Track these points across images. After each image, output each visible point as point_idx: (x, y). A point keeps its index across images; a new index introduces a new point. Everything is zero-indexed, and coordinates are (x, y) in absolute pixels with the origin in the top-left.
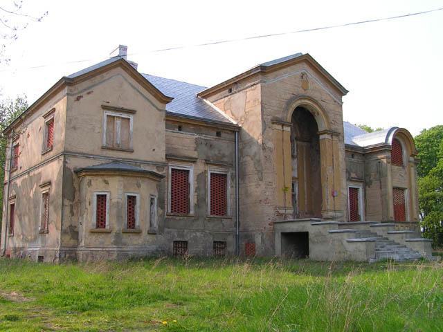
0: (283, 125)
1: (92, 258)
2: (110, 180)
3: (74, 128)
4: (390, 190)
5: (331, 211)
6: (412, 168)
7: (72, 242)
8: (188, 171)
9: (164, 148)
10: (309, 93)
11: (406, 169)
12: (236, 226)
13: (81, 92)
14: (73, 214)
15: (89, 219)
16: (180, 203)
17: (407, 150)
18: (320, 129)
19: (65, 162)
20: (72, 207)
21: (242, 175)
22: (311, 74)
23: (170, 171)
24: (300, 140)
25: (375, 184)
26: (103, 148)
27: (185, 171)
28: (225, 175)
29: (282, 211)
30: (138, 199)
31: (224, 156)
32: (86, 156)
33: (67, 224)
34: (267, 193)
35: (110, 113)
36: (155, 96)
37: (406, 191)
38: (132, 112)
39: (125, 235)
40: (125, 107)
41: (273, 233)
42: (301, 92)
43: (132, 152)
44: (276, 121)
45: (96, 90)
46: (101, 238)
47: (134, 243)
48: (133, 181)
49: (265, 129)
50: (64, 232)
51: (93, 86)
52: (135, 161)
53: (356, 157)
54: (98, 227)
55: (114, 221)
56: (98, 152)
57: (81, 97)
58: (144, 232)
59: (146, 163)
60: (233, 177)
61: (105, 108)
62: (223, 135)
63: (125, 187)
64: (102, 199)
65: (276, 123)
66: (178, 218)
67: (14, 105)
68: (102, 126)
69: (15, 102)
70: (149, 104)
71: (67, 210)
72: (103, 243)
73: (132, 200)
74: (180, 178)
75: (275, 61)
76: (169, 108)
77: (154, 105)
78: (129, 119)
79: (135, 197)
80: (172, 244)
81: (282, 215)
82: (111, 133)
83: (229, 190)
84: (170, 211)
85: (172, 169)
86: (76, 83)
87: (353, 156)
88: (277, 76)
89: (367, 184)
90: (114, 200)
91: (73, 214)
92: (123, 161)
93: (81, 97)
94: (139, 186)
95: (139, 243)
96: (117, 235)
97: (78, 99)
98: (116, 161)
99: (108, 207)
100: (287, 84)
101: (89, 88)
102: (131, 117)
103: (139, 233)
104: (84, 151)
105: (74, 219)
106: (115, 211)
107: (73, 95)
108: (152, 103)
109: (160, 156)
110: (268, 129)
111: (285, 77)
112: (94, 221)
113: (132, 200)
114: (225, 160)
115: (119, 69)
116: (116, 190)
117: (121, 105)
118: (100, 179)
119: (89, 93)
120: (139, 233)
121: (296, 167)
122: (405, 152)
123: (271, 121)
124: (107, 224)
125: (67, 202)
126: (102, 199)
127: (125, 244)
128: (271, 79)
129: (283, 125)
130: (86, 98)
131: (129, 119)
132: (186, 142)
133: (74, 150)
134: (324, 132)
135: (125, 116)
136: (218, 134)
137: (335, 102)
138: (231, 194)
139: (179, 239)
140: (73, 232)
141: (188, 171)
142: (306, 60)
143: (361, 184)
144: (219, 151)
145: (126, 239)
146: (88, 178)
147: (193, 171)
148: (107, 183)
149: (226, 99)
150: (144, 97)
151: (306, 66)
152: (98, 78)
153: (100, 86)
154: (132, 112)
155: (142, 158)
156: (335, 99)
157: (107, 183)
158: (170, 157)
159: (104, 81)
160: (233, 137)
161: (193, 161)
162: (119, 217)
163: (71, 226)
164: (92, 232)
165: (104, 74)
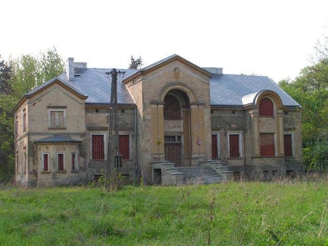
0: (157, 105)
1: (43, 186)
2: (49, 146)
3: (33, 120)
4: (256, 136)
5: (197, 154)
6: (280, 118)
7: (34, 178)
8: (103, 135)
9: (84, 125)
10: (180, 80)
11: (276, 119)
12: (135, 165)
13: (35, 101)
14: (34, 164)
15: (41, 166)
16: (98, 153)
17: (276, 104)
18: (191, 102)
19: (29, 138)
20: (33, 160)
21: (136, 137)
22: (182, 67)
23: (91, 137)
24: (184, 108)
25: (249, 131)
26: (49, 129)
27: (99, 136)
28: (128, 135)
29: (156, 156)
30: (64, 155)
31: (127, 124)
32: (39, 134)
33: (31, 169)
34: (148, 146)
35: (52, 110)
36: (79, 97)
37: (275, 135)
38: (65, 107)
39: (57, 174)
40: (60, 105)
41: (151, 169)
42: (174, 80)
43: (66, 129)
44: (152, 103)
45: (44, 98)
46: (46, 176)
47: (62, 177)
48: (61, 146)
49: (145, 109)
50: (30, 173)
51: (41, 97)
52: (69, 135)
53: (236, 112)
54: (45, 170)
55: (52, 167)
56: (47, 131)
57: (35, 103)
58: (68, 172)
59: (74, 134)
60: (133, 136)
61: (49, 107)
62: (126, 111)
63: (57, 150)
64: (46, 156)
65: (152, 104)
66: (97, 162)
67: (46, 58)
68: (48, 117)
69: (47, 55)
70: (74, 101)
71: (31, 162)
72: (47, 178)
73: (61, 156)
74: (98, 140)
75: (162, 60)
76: (87, 101)
77: (77, 102)
78: (63, 112)
79: (62, 154)
80: (93, 177)
81: (157, 158)
82: (53, 120)
83: (131, 144)
84: (91, 159)
85: (92, 135)
86: (33, 96)
87: (234, 112)
88: (154, 74)
89: (245, 131)
90: (52, 157)
91: (34, 164)
92: (60, 135)
93: (35, 103)
94: (64, 149)
95: (68, 176)
96: (54, 174)
97: (34, 105)
98: (56, 135)
99: (48, 160)
100: (161, 80)
101: (39, 98)
102: (64, 110)
103: (65, 172)
104: (39, 132)
105: (35, 166)
106: (52, 162)
107: (31, 103)
108: (76, 100)
109: (83, 129)
110: (147, 108)
111: (161, 73)
112: (43, 167)
113: (61, 156)
114: (128, 126)
115: (56, 85)
116: (53, 152)
117: (58, 104)
118: (45, 147)
119: (40, 101)
120: (65, 172)
121: (182, 125)
122: (275, 106)
123: (149, 102)
124: (49, 168)
125: (31, 158)
126: (46, 156)
127: (58, 178)
128: (149, 77)
129: (157, 105)
130: (38, 103)
131: (63, 112)
132: (101, 119)
133: (33, 132)
134: (194, 104)
135: (61, 110)
136: (123, 111)
137: (203, 82)
138: (132, 147)
139: (97, 174)
140: (34, 173)
141: (103, 135)
142: (177, 59)
143: (241, 131)
144: (124, 121)
145: (58, 175)
146: (39, 146)
147: (106, 135)
148: (47, 148)
149: (132, 87)
150: (72, 98)
151: (178, 62)
152: (44, 92)
153: (45, 96)
154: (65, 107)
155: (72, 132)
156: (203, 80)
157: (47, 148)
158: (90, 128)
159: (47, 93)
160: (133, 111)
161: (104, 129)
162: (54, 165)
163: (34, 170)
164: (42, 173)
165: (47, 89)
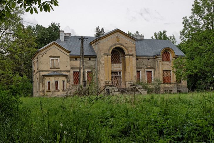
0: (108, 55)
4: (161, 72)
9: (69, 66)
10: (120, 42)
14: (43, 87)
15: (47, 88)
17: (172, 55)
18: (125, 54)
20: (42, 85)
23: (73, 72)
25: (157, 69)
30: (58, 82)
31: (92, 66)
37: (171, 71)
38: (59, 57)
40: (56, 56)
43: (59, 68)
48: (57, 77)
52: (61, 71)
53: (150, 59)
54: (48, 90)
57: (43, 55)
59: (64, 71)
61: (50, 57)
62: (91, 59)
64: (49, 82)
73: (57, 82)
76: (71, 53)
81: (107, 84)
86: (41, 51)
87: (149, 59)
92: (57, 71)
94: (59, 79)
97: (42, 56)
98: (54, 72)
101: (45, 52)
102: (59, 58)
109: (69, 68)
113: (57, 82)
115: (54, 45)
118: (48, 78)
120: (59, 91)
121: (121, 66)
122: (171, 56)
126: (49, 82)
129: (108, 55)
130: (45, 55)
135: (57, 58)
136: (90, 59)
137: (132, 43)
142: (118, 31)
143: (153, 69)
144: (90, 64)
145: (56, 93)
151: (118, 33)
154: (59, 57)
157: (50, 78)
160: (95, 59)
162: (53, 87)
